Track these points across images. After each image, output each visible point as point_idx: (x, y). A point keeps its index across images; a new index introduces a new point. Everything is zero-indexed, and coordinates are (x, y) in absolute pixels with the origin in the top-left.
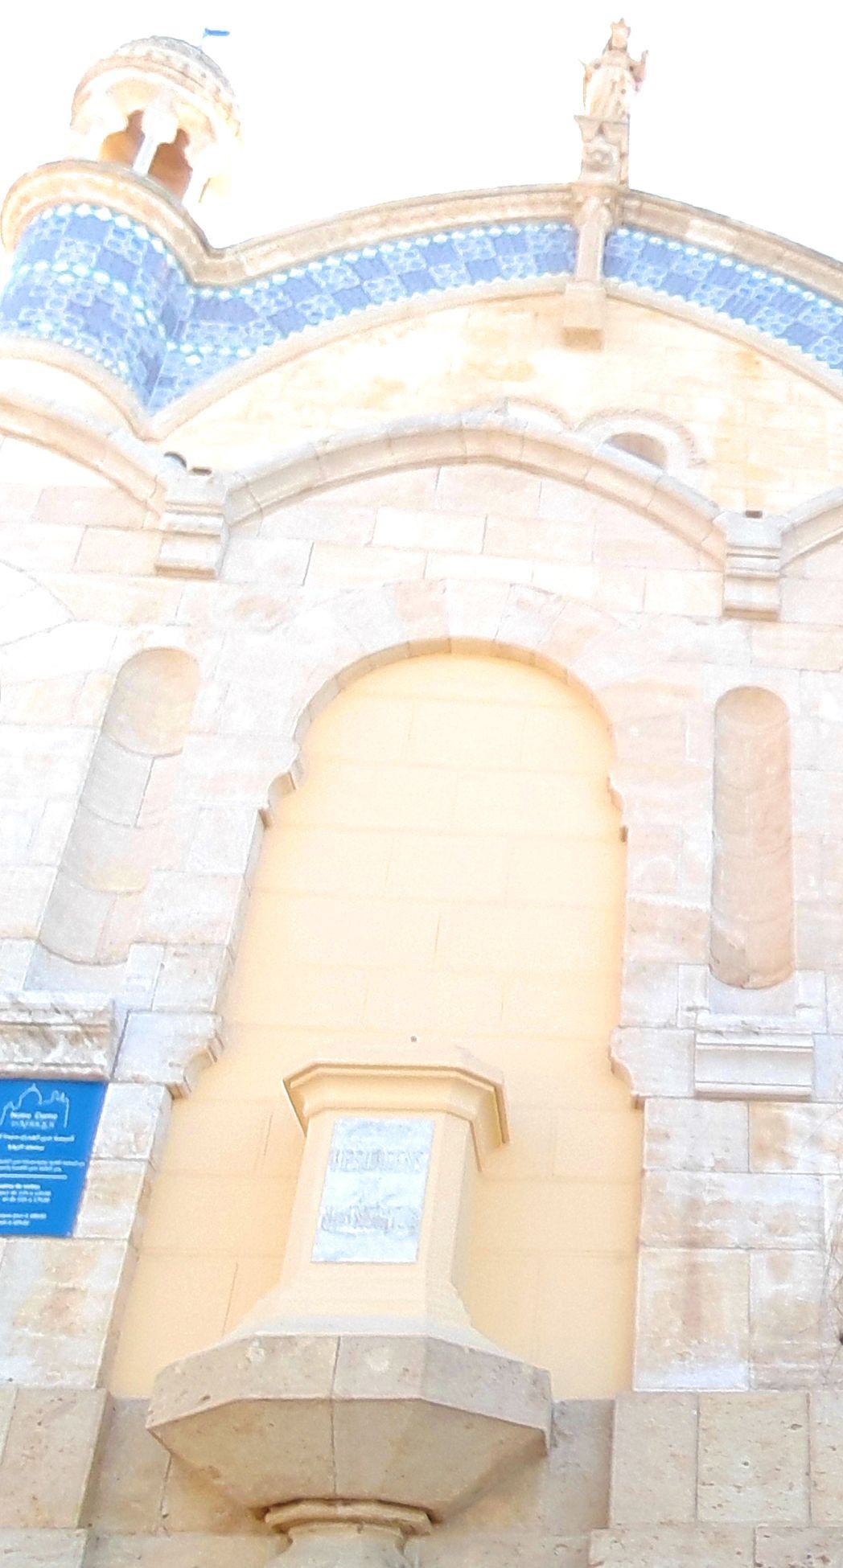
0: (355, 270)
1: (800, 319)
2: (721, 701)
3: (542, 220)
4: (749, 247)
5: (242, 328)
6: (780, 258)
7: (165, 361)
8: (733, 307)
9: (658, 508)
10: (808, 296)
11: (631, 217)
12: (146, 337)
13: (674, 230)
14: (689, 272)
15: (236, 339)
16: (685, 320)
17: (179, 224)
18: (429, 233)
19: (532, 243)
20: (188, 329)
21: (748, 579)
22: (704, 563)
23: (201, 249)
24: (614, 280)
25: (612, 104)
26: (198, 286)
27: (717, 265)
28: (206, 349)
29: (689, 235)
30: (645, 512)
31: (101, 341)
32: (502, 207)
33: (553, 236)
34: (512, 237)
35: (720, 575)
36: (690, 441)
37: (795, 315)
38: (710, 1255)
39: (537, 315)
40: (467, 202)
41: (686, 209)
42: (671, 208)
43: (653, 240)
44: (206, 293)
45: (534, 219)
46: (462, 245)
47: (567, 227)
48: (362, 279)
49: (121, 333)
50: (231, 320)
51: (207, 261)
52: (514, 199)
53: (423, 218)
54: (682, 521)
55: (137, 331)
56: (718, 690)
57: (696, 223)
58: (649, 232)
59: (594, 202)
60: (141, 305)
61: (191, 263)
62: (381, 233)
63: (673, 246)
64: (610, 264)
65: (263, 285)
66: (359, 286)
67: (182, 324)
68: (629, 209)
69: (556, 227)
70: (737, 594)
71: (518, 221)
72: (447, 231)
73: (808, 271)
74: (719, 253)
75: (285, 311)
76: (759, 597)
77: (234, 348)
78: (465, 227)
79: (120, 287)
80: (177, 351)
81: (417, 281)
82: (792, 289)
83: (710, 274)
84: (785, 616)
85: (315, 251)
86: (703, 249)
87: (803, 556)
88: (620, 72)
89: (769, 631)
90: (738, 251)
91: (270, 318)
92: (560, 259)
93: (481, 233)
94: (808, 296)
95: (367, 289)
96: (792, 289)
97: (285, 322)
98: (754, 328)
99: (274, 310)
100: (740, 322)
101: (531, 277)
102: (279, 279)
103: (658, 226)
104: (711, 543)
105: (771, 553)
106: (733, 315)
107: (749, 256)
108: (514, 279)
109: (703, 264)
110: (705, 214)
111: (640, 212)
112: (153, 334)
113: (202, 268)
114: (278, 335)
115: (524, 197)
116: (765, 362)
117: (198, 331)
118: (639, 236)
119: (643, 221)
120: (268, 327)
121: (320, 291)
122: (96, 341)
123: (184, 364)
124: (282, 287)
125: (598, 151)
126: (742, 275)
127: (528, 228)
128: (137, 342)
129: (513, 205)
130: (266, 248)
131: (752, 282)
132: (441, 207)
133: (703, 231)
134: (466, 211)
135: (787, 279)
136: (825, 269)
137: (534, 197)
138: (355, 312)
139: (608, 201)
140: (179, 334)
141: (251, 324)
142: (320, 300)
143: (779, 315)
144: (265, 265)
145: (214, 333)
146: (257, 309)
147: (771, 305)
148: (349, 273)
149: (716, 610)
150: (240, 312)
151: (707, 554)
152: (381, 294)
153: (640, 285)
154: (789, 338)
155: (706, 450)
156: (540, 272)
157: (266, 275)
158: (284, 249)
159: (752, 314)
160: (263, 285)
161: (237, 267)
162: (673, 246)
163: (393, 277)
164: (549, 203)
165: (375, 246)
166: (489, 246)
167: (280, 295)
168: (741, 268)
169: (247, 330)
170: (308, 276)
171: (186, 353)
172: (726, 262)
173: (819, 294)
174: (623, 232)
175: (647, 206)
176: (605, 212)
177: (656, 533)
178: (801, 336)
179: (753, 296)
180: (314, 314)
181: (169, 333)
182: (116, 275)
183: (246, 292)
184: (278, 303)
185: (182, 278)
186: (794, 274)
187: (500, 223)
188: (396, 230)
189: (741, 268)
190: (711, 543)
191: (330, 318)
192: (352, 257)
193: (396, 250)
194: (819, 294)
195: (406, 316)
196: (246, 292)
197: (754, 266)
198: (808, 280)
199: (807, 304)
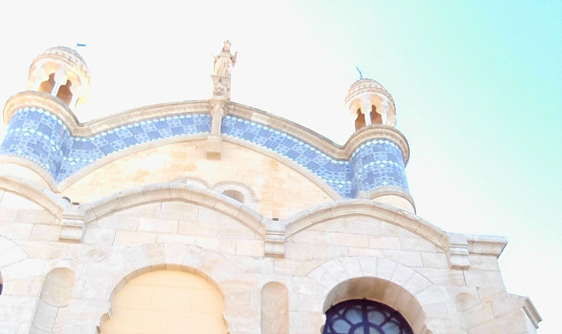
0: (131, 131)
1: (292, 149)
2: (264, 287)
3: (199, 113)
4: (274, 123)
5: (90, 152)
6: (285, 127)
7: (63, 164)
8: (268, 145)
9: (241, 217)
10: (295, 140)
11: (231, 112)
12: (56, 155)
13: (247, 117)
14: (252, 132)
15: (88, 156)
16: (251, 149)
17: (68, 115)
18: (158, 118)
19: (195, 121)
20: (71, 153)
21: (274, 243)
22: (258, 237)
23: (76, 123)
24: (225, 134)
25: (225, 71)
26: (75, 137)
27: (262, 129)
28: (77, 160)
29: (252, 118)
30: (236, 219)
31: (39, 157)
32: (185, 108)
33: (203, 119)
34: (188, 119)
35: (263, 241)
36: (252, 193)
37: (291, 147)
39: (197, 147)
40: (172, 106)
41: (251, 109)
42: (246, 108)
43: (239, 120)
44: (78, 139)
45: (196, 112)
46: (170, 122)
47: (208, 115)
48: (134, 134)
49: (47, 154)
50: (86, 149)
51: (78, 128)
52: (189, 105)
53: (156, 112)
54: (250, 222)
55: (53, 153)
56: (263, 283)
57: (255, 114)
58: (238, 117)
59: (218, 106)
60: (54, 144)
61: (72, 129)
62: (141, 118)
63: (246, 122)
64: (224, 129)
65: (98, 136)
66: (133, 137)
67: (69, 150)
68: (231, 109)
69: (204, 115)
70: (269, 248)
71: (190, 113)
72: (165, 117)
73: (295, 131)
74: (263, 125)
75: (106, 146)
76: (278, 249)
77: (88, 159)
79: (46, 137)
80: (67, 160)
81: (154, 135)
82: (289, 138)
83: (260, 133)
84: (287, 256)
85: (117, 124)
86: (257, 123)
88: (227, 59)
89: (281, 262)
90: (270, 124)
91: (101, 148)
92: (206, 127)
93: (177, 117)
94: (295, 140)
95: (136, 138)
96: (289, 138)
97: (106, 150)
98: (276, 152)
99: (102, 145)
100: (271, 150)
101: (195, 133)
102: (104, 134)
103: (241, 115)
104: (260, 230)
105: (282, 233)
106: (268, 147)
107: (274, 126)
108: (189, 134)
109: (257, 129)
110: (258, 111)
111: (234, 110)
112: (58, 154)
113: (76, 131)
114: (104, 155)
115: (192, 105)
116: (279, 164)
117: (74, 153)
118: (234, 119)
119: (236, 113)
120: (100, 152)
121: (119, 139)
122: (38, 157)
123: (69, 165)
124: (105, 137)
125: (219, 88)
126: (271, 133)
127: (194, 116)
128: (53, 157)
129: (189, 107)
130: (99, 123)
131: (275, 135)
132: (162, 108)
133: (257, 117)
134: (171, 110)
135: (288, 134)
136: (301, 131)
137: (196, 104)
138: (131, 146)
139: (223, 106)
140: (68, 154)
141: (94, 150)
142: (119, 142)
143: (285, 147)
144: (99, 129)
145: (81, 154)
146: (96, 145)
147: (282, 143)
148: (129, 132)
149: (262, 254)
150: (90, 146)
151: (259, 234)
152: (141, 140)
153: (234, 136)
154: (288, 156)
155: (259, 196)
156: (198, 132)
157: (99, 133)
158: (106, 123)
159: (275, 147)
160: (98, 136)
161: (89, 130)
162: (246, 122)
163: (145, 133)
164: (202, 107)
165: (139, 122)
166: (180, 122)
167: (104, 140)
168: (271, 130)
169: (92, 153)
170: (114, 133)
171: (70, 161)
172: (265, 128)
173: (299, 140)
174: (228, 117)
175: (237, 108)
176: (222, 110)
177: (241, 226)
178: (293, 155)
179: (275, 140)
180: (116, 147)
181: (64, 154)
182: (45, 132)
183: (92, 139)
184: (104, 143)
185: (69, 134)
186: (290, 132)
187: (183, 114)
188: (146, 117)
189: (271, 130)
190: (260, 230)
191: (122, 148)
192: (130, 126)
193: (146, 124)
194: (299, 140)
195: (150, 147)
196: (92, 139)
197: (275, 130)
198: (295, 135)
199: (295, 143)
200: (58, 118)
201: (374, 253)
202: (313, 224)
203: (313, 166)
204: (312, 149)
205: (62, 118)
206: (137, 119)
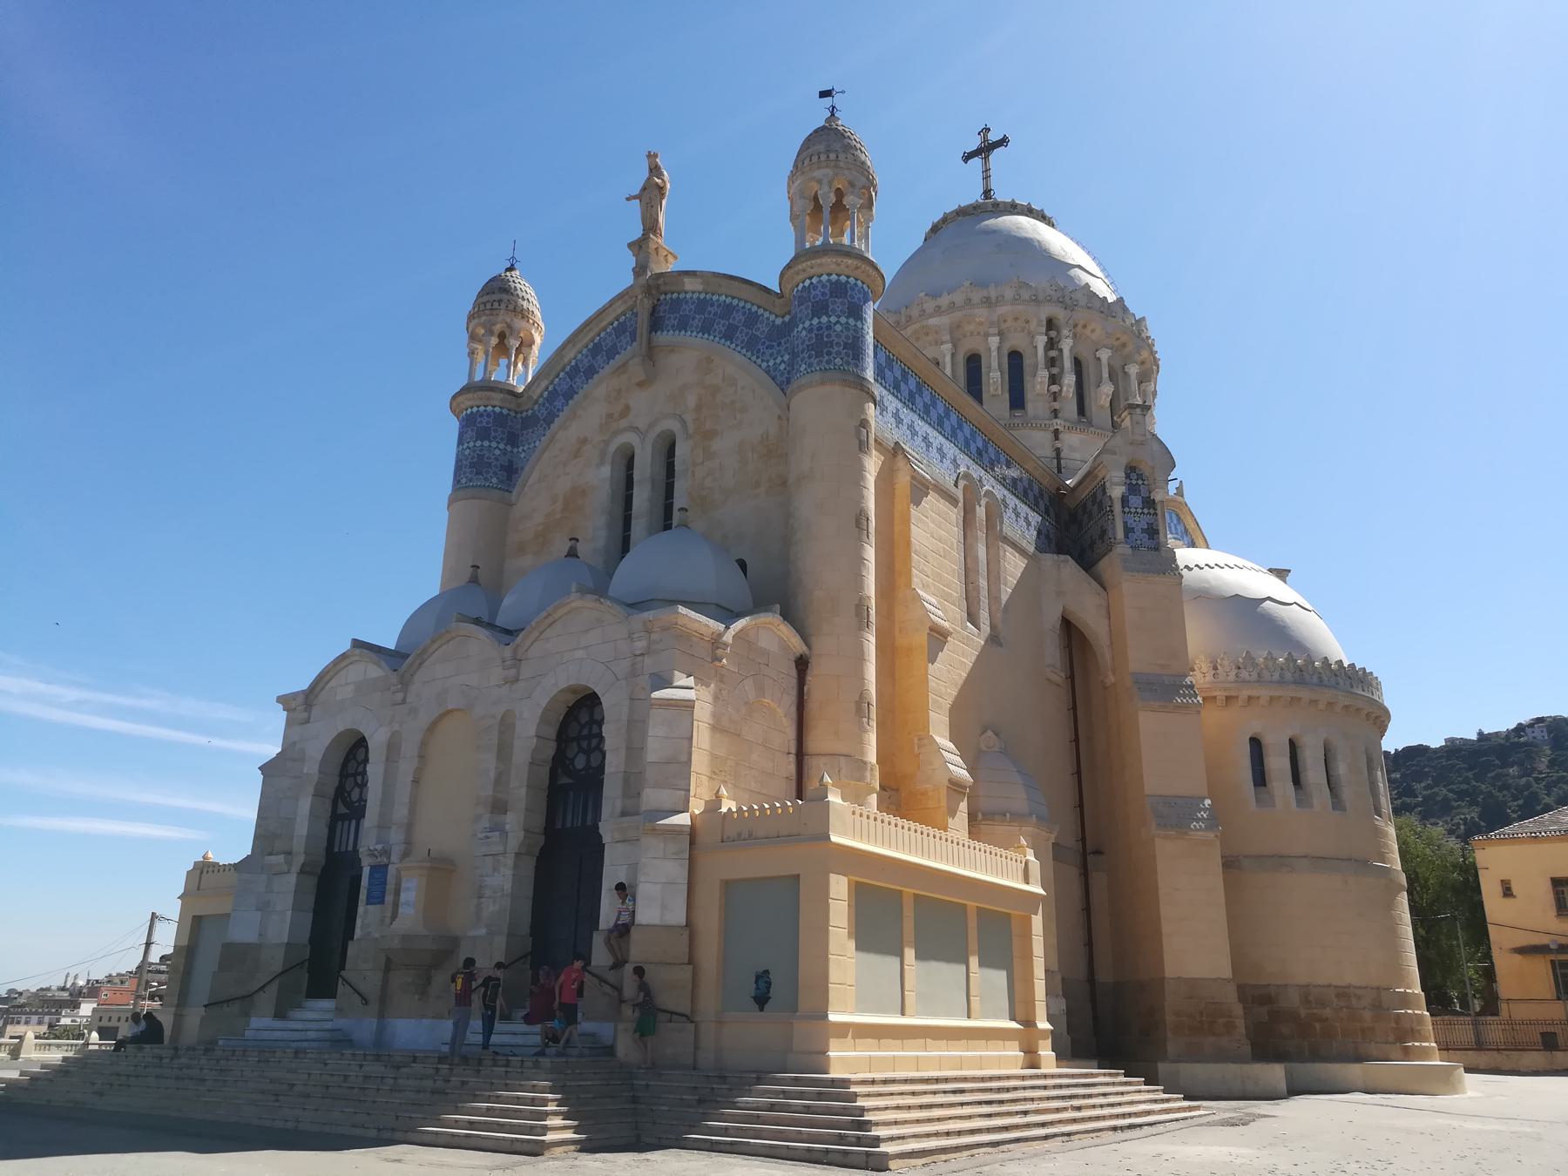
18: (592, 340)
38: (482, 900)
44: (524, 414)
51: (519, 401)
52: (617, 304)
57: (687, 280)
61: (513, 406)
78: (604, 329)
87: (526, 651)
97: (549, 421)
110: (687, 273)
144: (539, 391)
157: (541, 395)
161: (530, 397)
174: (662, 297)
178: (729, 335)
181: (513, 446)
196: (536, 407)
200: (494, 407)
201: (580, 654)
202: (541, 634)
203: (751, 345)
204: (754, 309)
205: (497, 404)
206: (572, 355)
